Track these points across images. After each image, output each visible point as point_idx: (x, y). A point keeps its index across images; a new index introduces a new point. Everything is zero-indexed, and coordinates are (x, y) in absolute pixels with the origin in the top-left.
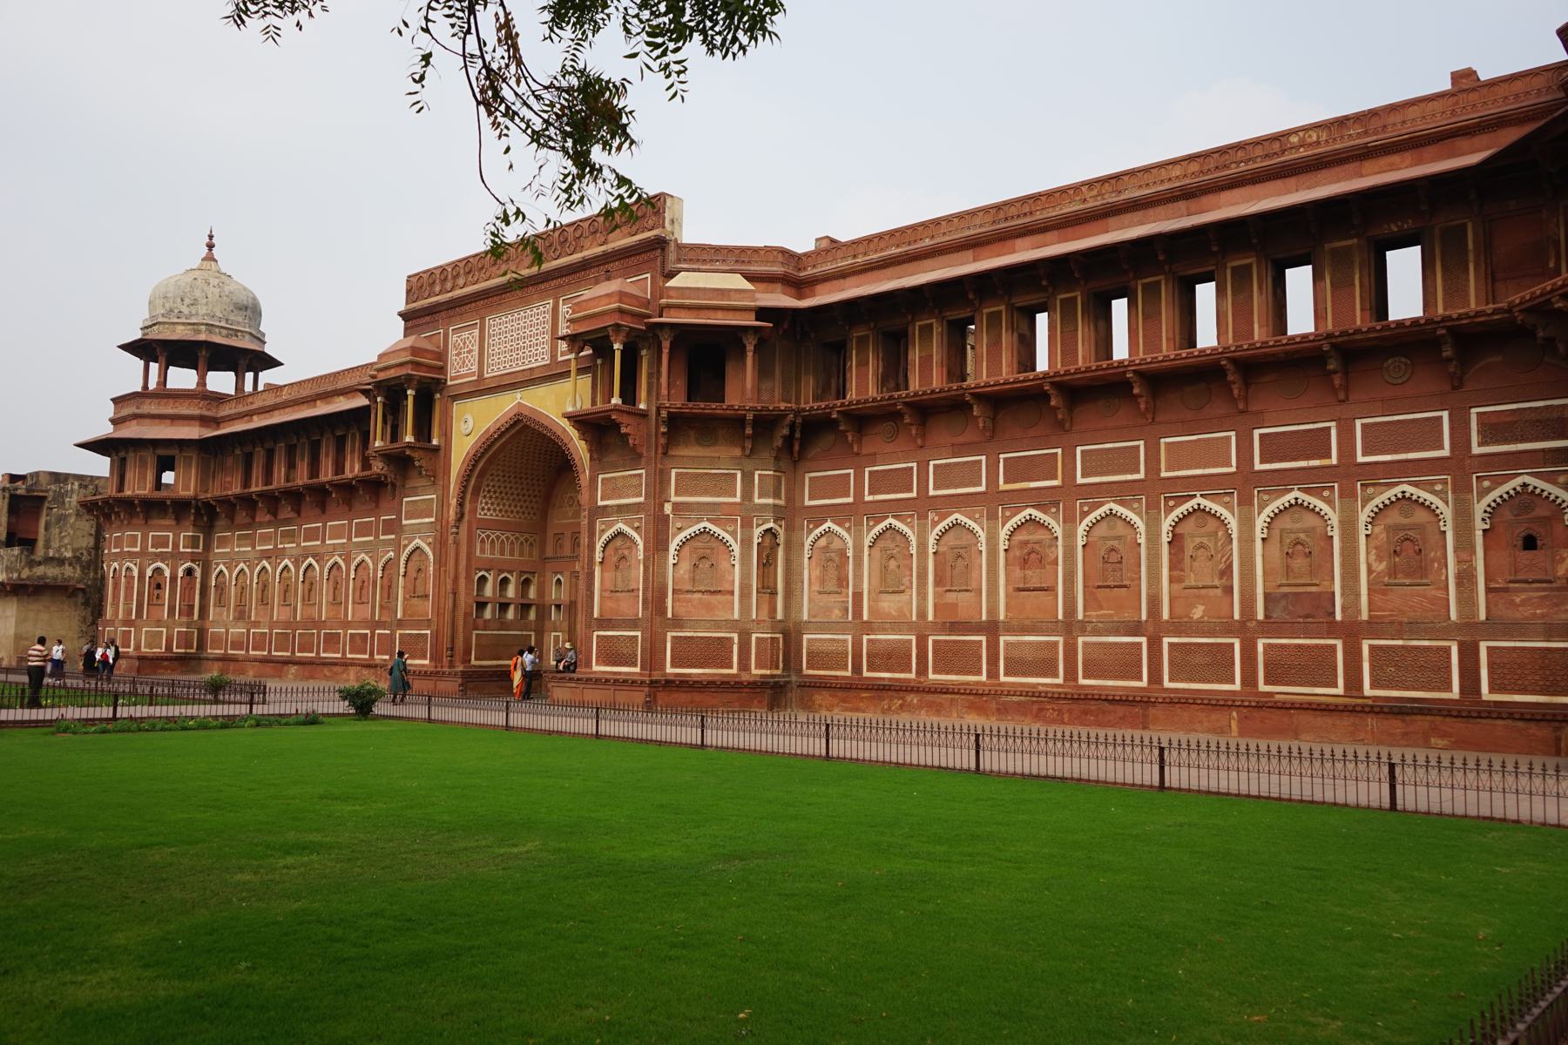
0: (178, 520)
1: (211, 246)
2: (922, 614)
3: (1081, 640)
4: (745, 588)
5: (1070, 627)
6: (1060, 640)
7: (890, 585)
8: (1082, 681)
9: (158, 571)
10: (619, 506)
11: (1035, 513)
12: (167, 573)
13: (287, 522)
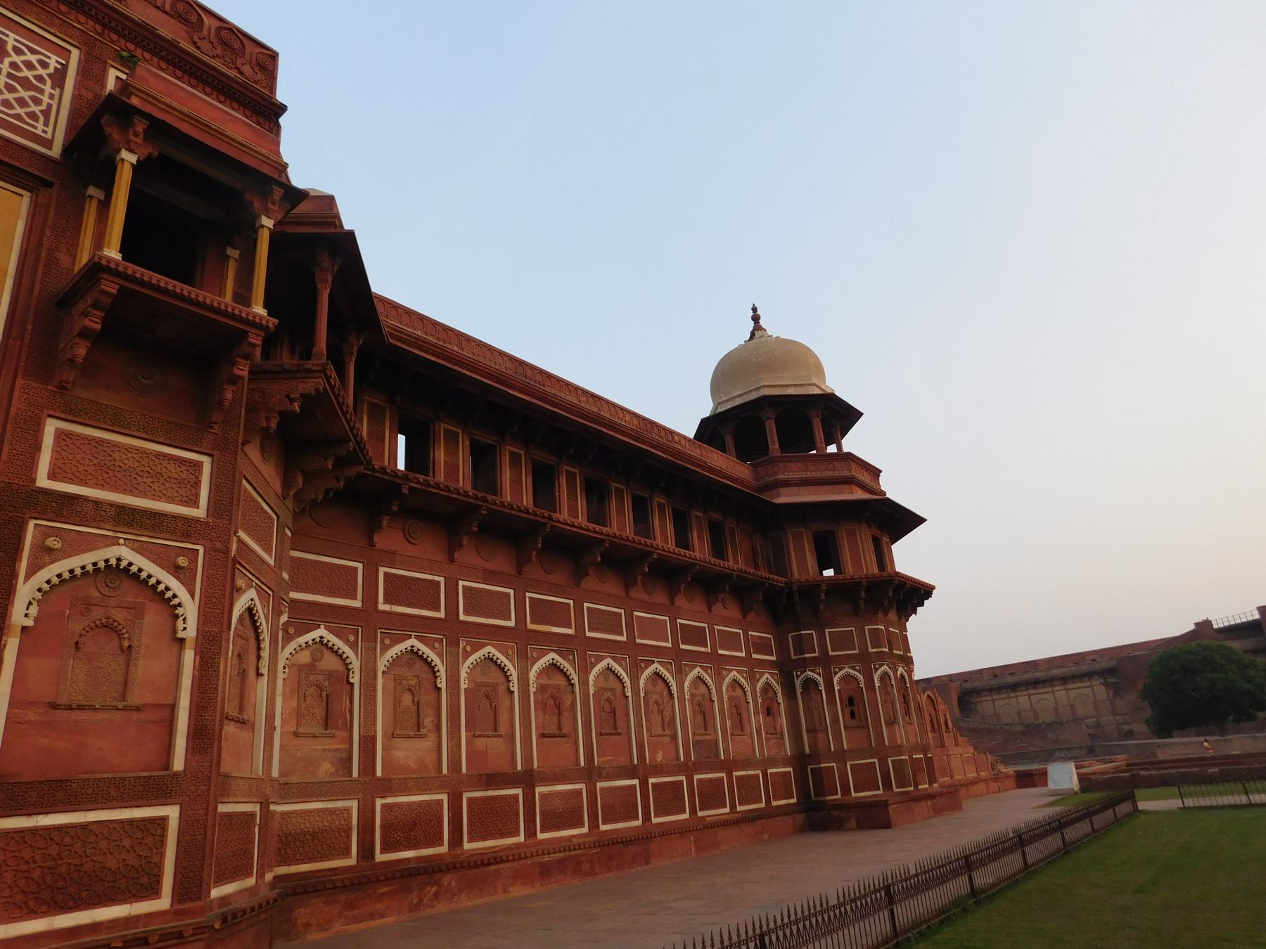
2: (455, 765)
3: (599, 785)
4: (270, 717)
5: (591, 774)
6: (582, 786)
7: (410, 724)
8: (603, 828)
10: (122, 509)
11: (557, 658)
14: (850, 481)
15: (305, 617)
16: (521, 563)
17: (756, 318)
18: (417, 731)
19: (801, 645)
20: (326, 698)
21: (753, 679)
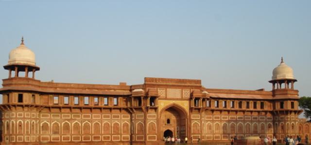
0: (37, 110)
1: (23, 41)
9: (33, 122)
12: (35, 123)
13: (77, 113)
14: (287, 94)
15: (207, 121)
16: (229, 113)
17: (282, 60)
18: (218, 129)
19: (276, 119)
20: (210, 127)
21: (266, 123)
